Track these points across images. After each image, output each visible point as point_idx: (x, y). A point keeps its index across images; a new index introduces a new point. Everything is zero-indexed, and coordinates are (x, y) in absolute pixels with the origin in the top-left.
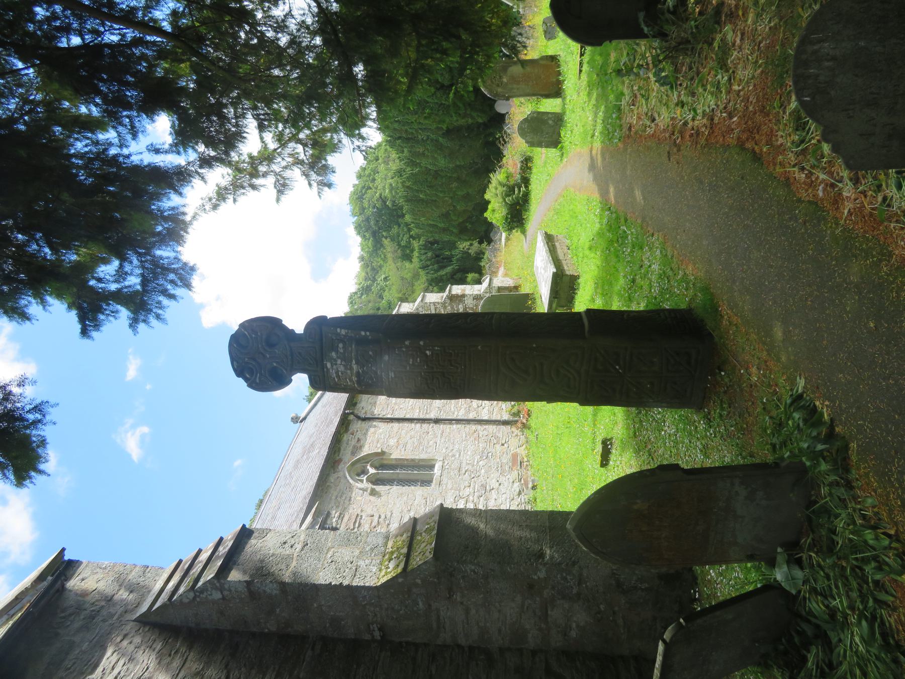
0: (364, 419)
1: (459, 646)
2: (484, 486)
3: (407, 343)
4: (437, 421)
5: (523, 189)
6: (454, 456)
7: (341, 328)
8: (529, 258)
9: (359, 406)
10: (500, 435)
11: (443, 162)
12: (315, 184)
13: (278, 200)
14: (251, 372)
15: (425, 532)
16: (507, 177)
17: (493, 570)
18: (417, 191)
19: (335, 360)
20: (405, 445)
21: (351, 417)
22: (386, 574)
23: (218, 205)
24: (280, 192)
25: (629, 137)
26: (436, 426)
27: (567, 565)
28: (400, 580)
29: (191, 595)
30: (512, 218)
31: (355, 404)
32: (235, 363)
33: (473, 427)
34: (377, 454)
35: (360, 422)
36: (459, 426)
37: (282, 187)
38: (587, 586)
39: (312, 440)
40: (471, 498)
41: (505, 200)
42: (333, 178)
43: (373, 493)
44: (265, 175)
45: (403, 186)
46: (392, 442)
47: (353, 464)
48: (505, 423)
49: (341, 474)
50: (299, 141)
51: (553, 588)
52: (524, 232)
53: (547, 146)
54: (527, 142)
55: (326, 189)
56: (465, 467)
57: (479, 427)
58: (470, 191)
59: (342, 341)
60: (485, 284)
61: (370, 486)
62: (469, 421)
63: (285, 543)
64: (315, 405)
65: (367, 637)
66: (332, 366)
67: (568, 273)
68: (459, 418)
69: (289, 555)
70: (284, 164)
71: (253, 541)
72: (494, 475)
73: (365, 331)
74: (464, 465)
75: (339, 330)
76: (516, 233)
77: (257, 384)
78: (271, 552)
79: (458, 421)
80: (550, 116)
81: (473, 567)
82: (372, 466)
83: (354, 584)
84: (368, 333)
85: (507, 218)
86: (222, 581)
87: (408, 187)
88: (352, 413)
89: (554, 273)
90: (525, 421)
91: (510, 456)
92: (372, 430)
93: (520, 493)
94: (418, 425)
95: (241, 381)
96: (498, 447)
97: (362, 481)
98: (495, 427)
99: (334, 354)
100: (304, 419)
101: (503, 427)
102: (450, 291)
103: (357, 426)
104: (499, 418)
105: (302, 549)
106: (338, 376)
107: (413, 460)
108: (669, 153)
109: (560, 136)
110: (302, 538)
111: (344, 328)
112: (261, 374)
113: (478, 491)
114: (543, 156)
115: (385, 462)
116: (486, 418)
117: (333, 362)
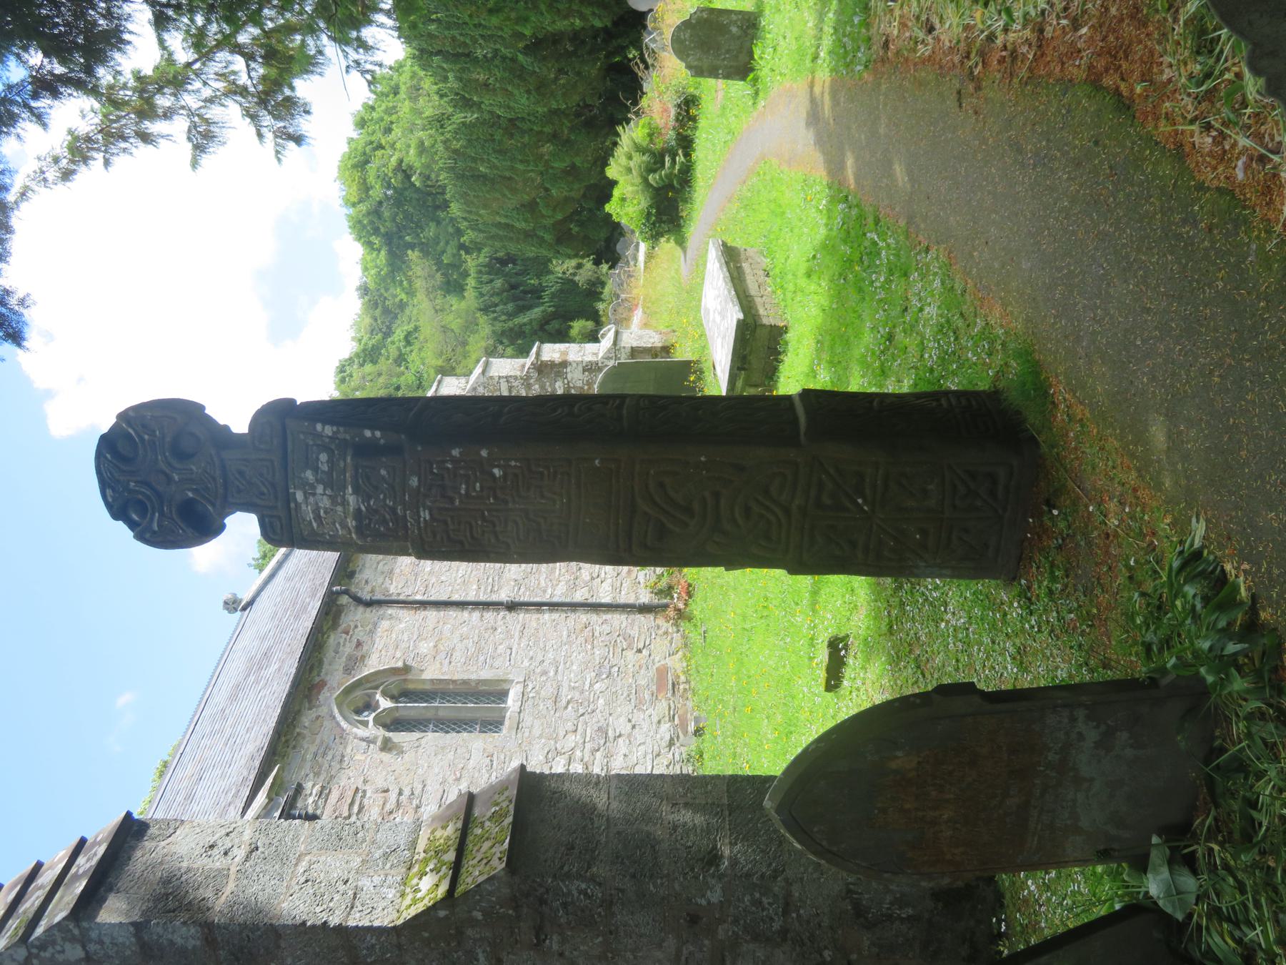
0: (370, 604)
2: (603, 731)
3: (455, 452)
4: (512, 606)
5: (680, 158)
6: (545, 673)
7: (324, 423)
8: (692, 293)
10: (634, 632)
11: (524, 101)
12: (269, 136)
13: (195, 164)
14: (143, 510)
15: (490, 819)
16: (650, 135)
17: (622, 891)
18: (474, 160)
19: (314, 488)
20: (450, 654)
22: (415, 901)
23: (73, 172)
24: (199, 149)
25: (883, 61)
26: (511, 617)
28: (442, 913)
29: (22, 953)
30: (659, 213)
31: (351, 575)
32: (109, 492)
33: (583, 617)
34: (394, 671)
35: (361, 609)
36: (555, 616)
37: (203, 138)
38: (799, 916)
39: (266, 645)
40: (578, 753)
41: (646, 180)
42: (303, 124)
43: (387, 746)
44: (168, 115)
45: (447, 148)
46: (425, 647)
47: (348, 691)
48: (644, 609)
49: (323, 711)
50: (238, 49)
51: (736, 921)
52: (681, 242)
53: (728, 76)
54: (689, 67)
55: (291, 145)
56: (566, 695)
57: (594, 618)
58: (578, 161)
59: (325, 448)
60: (606, 343)
61: (381, 732)
62: (574, 606)
63: (212, 847)
64: (272, 576)
66: (306, 498)
67: (765, 321)
68: (555, 599)
69: (220, 871)
70: (207, 93)
71: (148, 844)
72: (624, 709)
73: (372, 428)
74: (564, 691)
75: (319, 427)
76: (667, 246)
77: (155, 532)
78: (185, 864)
79: (554, 606)
80: (734, 17)
81: (583, 886)
82: (384, 694)
83: (351, 923)
84: (378, 434)
85: (649, 214)
86: (85, 924)
87: (456, 151)
88: (346, 592)
89: (739, 321)
90: (681, 606)
91: (652, 672)
92: (385, 624)
93: (671, 744)
94: (476, 615)
96: (630, 654)
97: (365, 724)
98: (624, 617)
99: (309, 475)
100: (250, 603)
101: (640, 618)
103: (355, 616)
104: (631, 600)
105: (247, 858)
106: (318, 517)
107: (465, 682)
108: (959, 92)
109: (752, 57)
110: (247, 836)
111: (332, 423)
112: (162, 514)
113: (592, 739)
114: (718, 94)
115: (411, 686)
116: (606, 599)
117: (309, 491)
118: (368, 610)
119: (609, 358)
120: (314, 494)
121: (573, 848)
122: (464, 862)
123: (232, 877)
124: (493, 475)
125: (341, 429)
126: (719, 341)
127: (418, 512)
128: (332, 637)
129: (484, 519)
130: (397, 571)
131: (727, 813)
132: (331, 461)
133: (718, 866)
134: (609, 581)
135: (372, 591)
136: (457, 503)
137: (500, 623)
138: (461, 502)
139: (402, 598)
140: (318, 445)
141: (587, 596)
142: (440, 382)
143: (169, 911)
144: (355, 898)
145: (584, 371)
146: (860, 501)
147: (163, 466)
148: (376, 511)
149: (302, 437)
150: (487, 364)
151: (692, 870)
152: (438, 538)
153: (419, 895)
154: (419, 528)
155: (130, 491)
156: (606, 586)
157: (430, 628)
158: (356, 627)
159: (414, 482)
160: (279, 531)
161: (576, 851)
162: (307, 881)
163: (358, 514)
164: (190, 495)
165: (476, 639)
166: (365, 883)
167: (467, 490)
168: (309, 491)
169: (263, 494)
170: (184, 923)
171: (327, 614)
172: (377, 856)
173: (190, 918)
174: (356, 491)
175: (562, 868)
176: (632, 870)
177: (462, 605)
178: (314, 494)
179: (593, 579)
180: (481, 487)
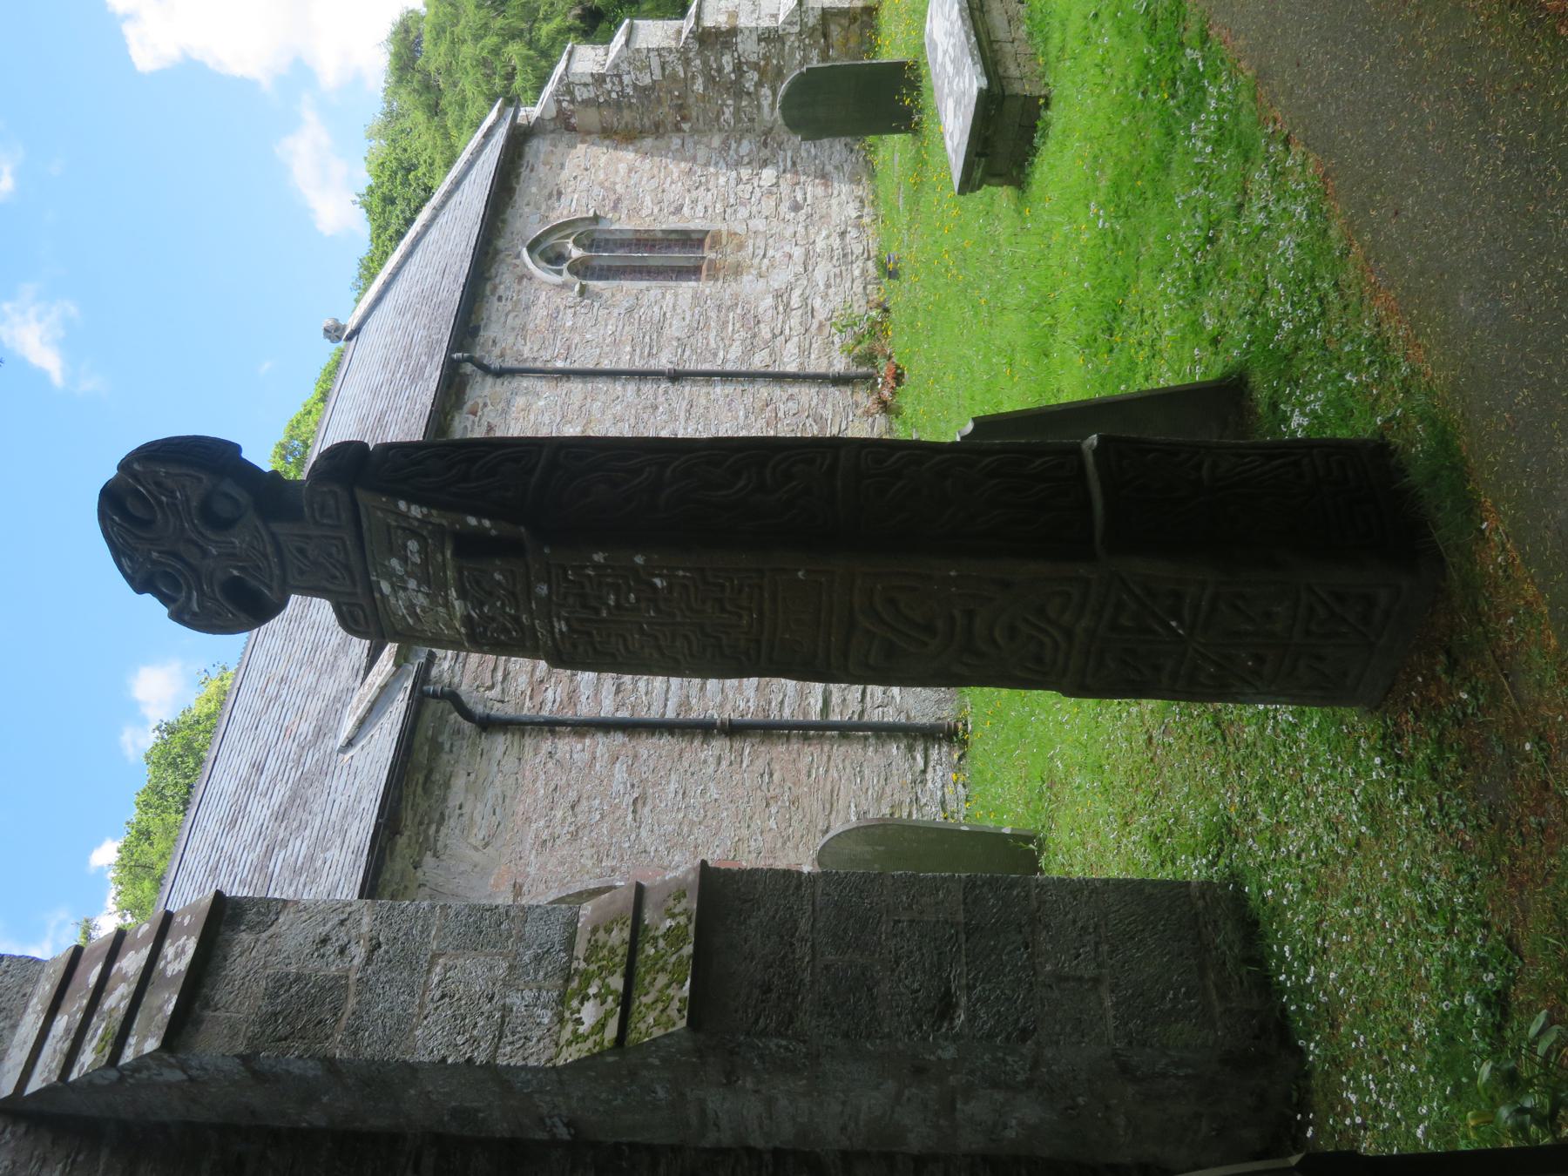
0: (501, 373)
1: (750, 1151)
3: (599, 557)
4: (676, 377)
7: (410, 500)
9: (486, 335)
10: (827, 413)
21: (468, 368)
22: (577, 1038)
26: (673, 389)
27: (1008, 1039)
33: (764, 391)
35: (489, 380)
36: (729, 389)
39: (380, 405)
57: (778, 392)
59: (414, 533)
62: (752, 376)
63: (324, 941)
65: (541, 1135)
67: (1017, 88)
68: (729, 367)
69: (336, 979)
73: (479, 514)
75: (402, 505)
77: (194, 614)
78: (293, 969)
79: (727, 376)
81: (784, 1043)
84: (487, 523)
88: (471, 360)
89: (980, 91)
90: (886, 394)
92: (520, 401)
94: (631, 387)
95: (149, 599)
98: (814, 391)
99: (395, 562)
100: (356, 332)
101: (836, 394)
102: (698, 17)
103: (483, 391)
104: (822, 370)
105: (369, 960)
110: (365, 929)
111: (421, 503)
116: (792, 368)
117: (399, 585)
118: (499, 381)
119: (791, 24)
120: (405, 589)
121: (769, 990)
122: (635, 994)
123: (353, 989)
124: (654, 586)
125: (434, 512)
126: (950, 104)
127: (551, 623)
128: (457, 419)
129: (642, 632)
130: (532, 326)
131: (963, 937)
132: (423, 550)
133: (952, 1020)
134: (795, 339)
135: (502, 355)
136: (604, 614)
137: (661, 399)
138: (610, 613)
139: (539, 365)
140: (404, 529)
141: (768, 360)
142: (571, 54)
143: (280, 1040)
144: (503, 1022)
145: (760, 40)
146: (1174, 624)
147: (194, 536)
148: (493, 619)
149: (379, 514)
150: (631, 31)
151: (920, 1026)
152: (581, 649)
153: (581, 1029)
154: (554, 639)
155: (154, 562)
156: (792, 347)
157: (578, 404)
158: (485, 405)
159: (543, 590)
160: (362, 621)
161: (774, 996)
162: (443, 997)
163: (467, 620)
164: (235, 573)
165: (632, 421)
166: (514, 999)
167: (617, 600)
168: (399, 585)
169: (334, 577)
170: (300, 1057)
171: (449, 387)
172: (526, 959)
173: (306, 1050)
174: (463, 595)
175: (756, 1022)
176: (844, 1027)
177: (613, 375)
178: (405, 589)
179: (775, 336)
180: (638, 599)
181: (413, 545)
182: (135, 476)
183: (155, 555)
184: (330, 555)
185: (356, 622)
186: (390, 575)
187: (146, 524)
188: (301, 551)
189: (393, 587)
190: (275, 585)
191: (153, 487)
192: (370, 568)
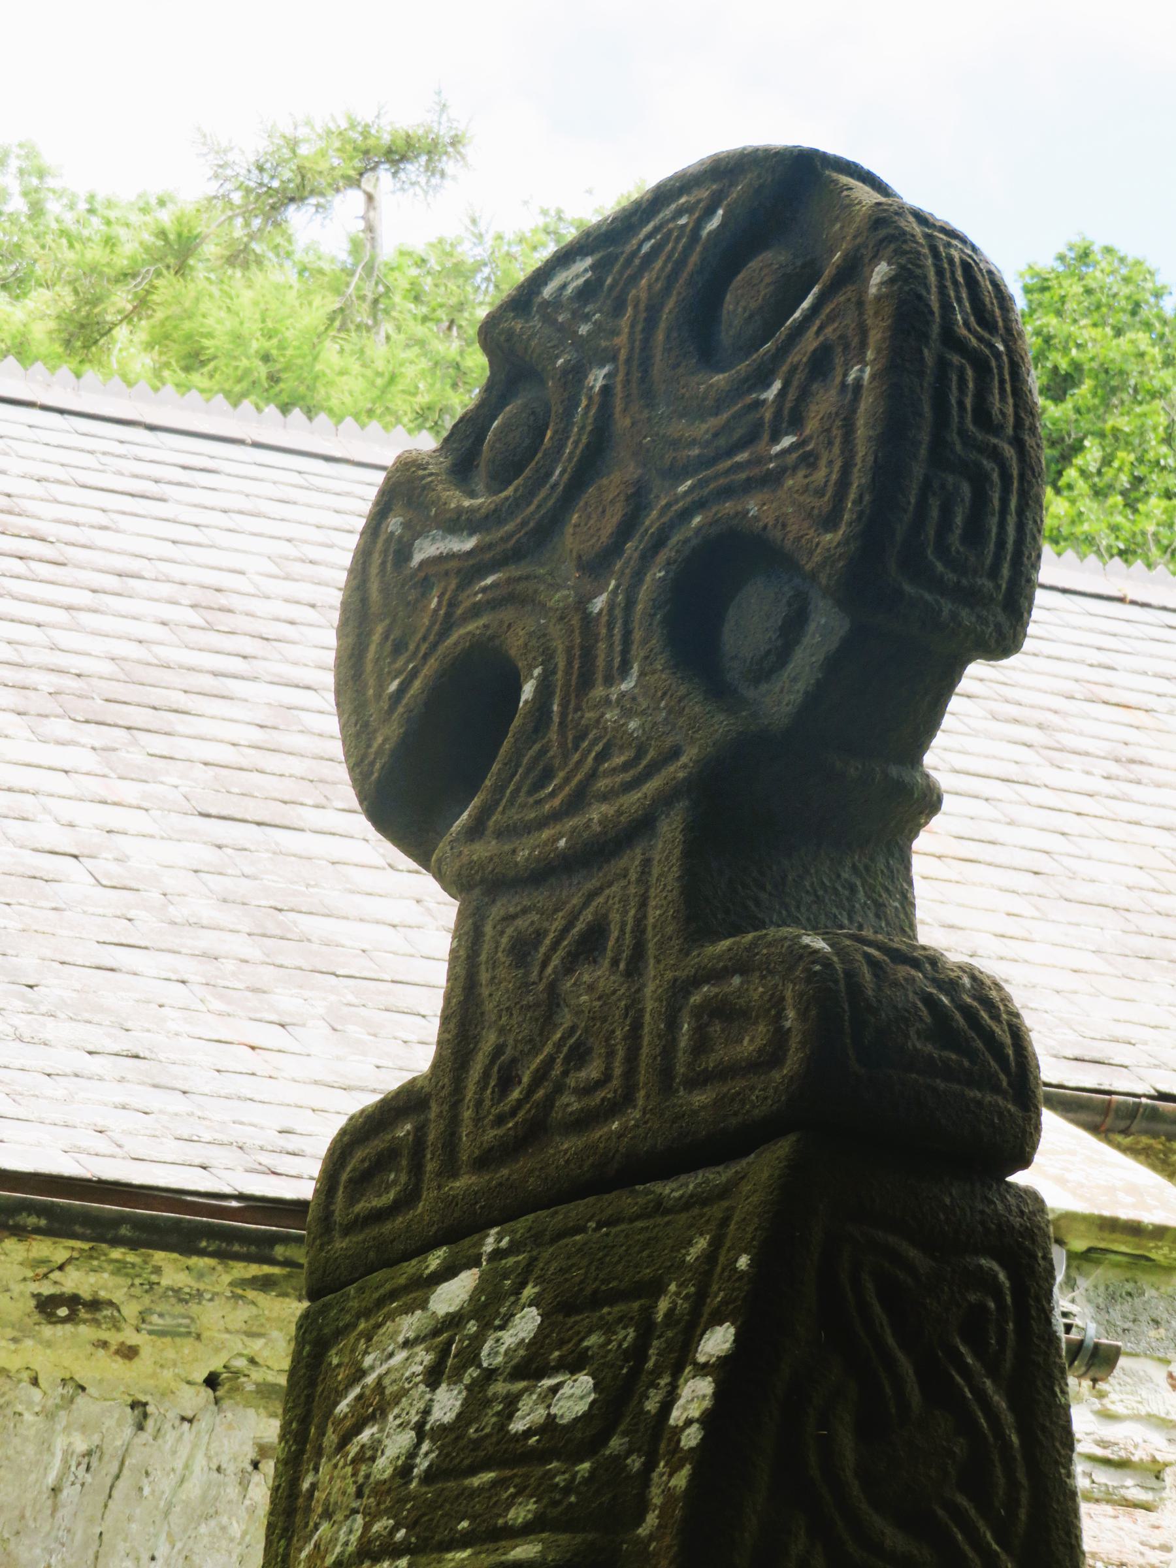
32: (580, 270)
75: (717, 1342)
77: (403, 553)
99: (526, 1323)
112: (470, 569)
120: (434, 1377)
125: (680, 1480)
140: (638, 1352)
147: (652, 520)
155: (576, 374)
160: (361, 1207)
164: (528, 691)
169: (507, 1081)
178: (434, 1377)
181: (575, 1395)
182: (852, 271)
183: (597, 378)
184: (578, 1056)
185: (363, 1180)
186: (488, 1310)
187: (701, 333)
188: (591, 943)
189: (454, 1321)
190: (482, 850)
191: (810, 343)
192: (522, 1224)
